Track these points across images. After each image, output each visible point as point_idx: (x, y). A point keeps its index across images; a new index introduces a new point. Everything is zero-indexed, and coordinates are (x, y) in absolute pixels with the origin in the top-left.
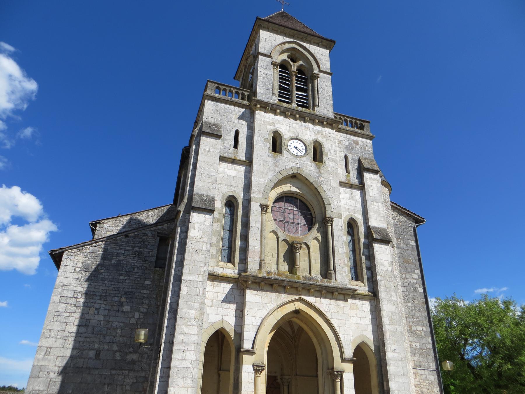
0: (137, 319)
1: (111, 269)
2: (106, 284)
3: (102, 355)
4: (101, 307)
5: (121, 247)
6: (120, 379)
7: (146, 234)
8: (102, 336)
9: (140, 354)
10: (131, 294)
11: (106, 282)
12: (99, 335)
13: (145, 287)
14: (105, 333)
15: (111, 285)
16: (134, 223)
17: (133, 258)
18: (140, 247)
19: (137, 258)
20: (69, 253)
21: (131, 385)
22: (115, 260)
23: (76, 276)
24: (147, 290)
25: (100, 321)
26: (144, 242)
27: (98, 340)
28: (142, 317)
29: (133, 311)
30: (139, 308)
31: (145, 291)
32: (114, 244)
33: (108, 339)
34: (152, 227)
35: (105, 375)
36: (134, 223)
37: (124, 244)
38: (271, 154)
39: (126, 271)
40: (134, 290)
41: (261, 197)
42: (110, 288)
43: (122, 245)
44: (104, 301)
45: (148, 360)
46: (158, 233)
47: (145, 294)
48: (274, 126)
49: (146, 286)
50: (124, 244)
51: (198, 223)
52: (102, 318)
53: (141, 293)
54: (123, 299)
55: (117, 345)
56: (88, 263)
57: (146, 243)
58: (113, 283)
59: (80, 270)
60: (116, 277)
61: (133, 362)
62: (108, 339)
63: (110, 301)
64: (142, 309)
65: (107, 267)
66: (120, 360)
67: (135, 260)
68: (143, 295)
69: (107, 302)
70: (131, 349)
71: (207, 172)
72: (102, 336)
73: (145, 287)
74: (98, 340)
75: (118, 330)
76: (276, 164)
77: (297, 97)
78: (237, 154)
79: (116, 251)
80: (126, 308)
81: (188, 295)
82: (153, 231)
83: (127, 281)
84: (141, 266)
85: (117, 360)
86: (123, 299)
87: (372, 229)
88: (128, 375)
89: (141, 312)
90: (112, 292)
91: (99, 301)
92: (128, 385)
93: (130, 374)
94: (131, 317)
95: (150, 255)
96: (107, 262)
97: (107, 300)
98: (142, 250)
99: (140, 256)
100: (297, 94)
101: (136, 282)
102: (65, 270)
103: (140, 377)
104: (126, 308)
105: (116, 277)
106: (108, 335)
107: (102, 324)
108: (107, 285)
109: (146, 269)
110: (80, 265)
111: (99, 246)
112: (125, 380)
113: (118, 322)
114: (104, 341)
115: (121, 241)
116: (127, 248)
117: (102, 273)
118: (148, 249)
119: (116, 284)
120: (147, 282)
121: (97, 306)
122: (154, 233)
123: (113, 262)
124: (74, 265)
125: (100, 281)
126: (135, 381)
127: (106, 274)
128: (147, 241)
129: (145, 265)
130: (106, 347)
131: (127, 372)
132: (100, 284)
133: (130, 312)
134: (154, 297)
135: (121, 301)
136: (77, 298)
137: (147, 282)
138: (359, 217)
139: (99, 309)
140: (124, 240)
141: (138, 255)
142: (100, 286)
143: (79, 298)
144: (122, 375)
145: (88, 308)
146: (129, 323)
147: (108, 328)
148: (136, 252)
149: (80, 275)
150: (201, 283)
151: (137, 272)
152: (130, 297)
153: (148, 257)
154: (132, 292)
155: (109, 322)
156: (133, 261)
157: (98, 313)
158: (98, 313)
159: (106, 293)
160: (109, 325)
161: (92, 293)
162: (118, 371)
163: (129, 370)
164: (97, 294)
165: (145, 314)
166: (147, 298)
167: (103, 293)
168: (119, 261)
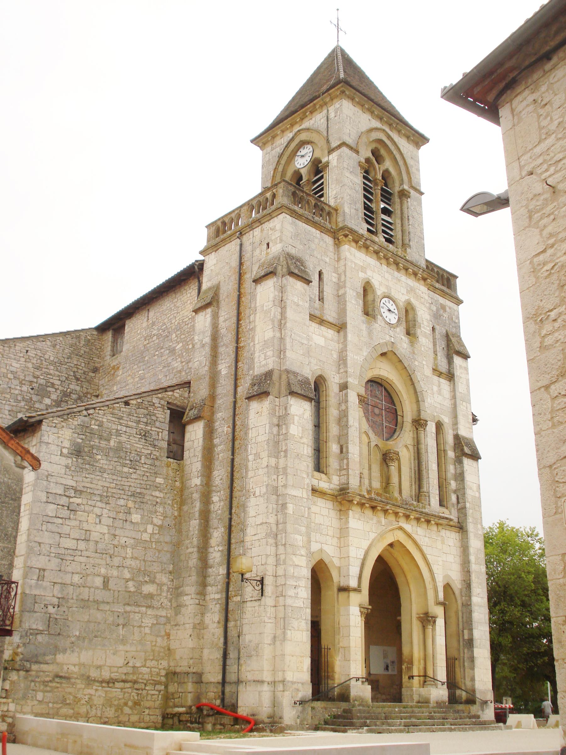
0: (151, 534)
1: (111, 454)
2: (106, 478)
3: (111, 585)
4: (104, 513)
5: (121, 421)
6: (137, 618)
7: (152, 404)
8: (108, 556)
9: (158, 585)
10: (140, 496)
11: (105, 475)
12: (104, 555)
13: (157, 487)
14: (111, 552)
15: (113, 480)
16: (34, 356)
17: (139, 441)
18: (146, 424)
19: (143, 441)
20: (51, 424)
21: (151, 627)
22: (115, 441)
23: (65, 461)
24: (160, 491)
25: (104, 534)
26: (150, 415)
27: (103, 562)
28: (157, 532)
29: (144, 522)
30: (152, 518)
31: (157, 494)
32: (111, 415)
33: (116, 561)
34: (160, 393)
35: (117, 611)
36: (34, 356)
37: (125, 415)
38: (364, 318)
39: (131, 461)
40: (143, 490)
41: (357, 383)
42: (113, 485)
43: (121, 418)
44: (107, 503)
45: (169, 593)
46: (168, 403)
47: (157, 497)
48: (365, 273)
49: (158, 485)
50: (125, 415)
51: (296, 415)
52: (105, 530)
53: (152, 495)
54: (130, 504)
55: (129, 572)
56: (78, 443)
57: (154, 418)
58: (115, 477)
59: (68, 453)
60: (119, 468)
61: (151, 596)
62: (116, 561)
63: (113, 506)
64: (155, 521)
65: (105, 451)
66: (134, 592)
67: (141, 443)
68: (155, 498)
69: (110, 506)
70: (147, 577)
71: (298, 338)
72: (108, 556)
73: (157, 487)
74: (103, 562)
75: (128, 549)
76: (370, 333)
77: (383, 225)
78: (323, 310)
79: (114, 427)
80: (136, 517)
81: (295, 516)
82: (161, 399)
83: (134, 476)
84: (150, 454)
85: (130, 592)
86: (130, 504)
87: (461, 440)
88: (146, 614)
89: (155, 525)
90: (114, 491)
91: (99, 504)
92: (147, 627)
93: (149, 613)
94: (143, 531)
95: (160, 437)
96: (104, 443)
97: (109, 504)
98: (149, 428)
99: (147, 438)
100: (383, 220)
101: (145, 478)
102: (47, 450)
103: (161, 616)
104: (136, 517)
105: (119, 468)
106: (116, 556)
107: (106, 538)
108: (108, 480)
109: (157, 459)
110: (67, 444)
111: (91, 416)
112: (143, 621)
113: (127, 537)
114: (112, 564)
115: (120, 410)
116: (130, 423)
117: (99, 459)
118: (156, 427)
119: (120, 479)
120: (159, 480)
121: (97, 511)
122: (163, 402)
123: (112, 443)
124: (60, 444)
125: (98, 473)
126: (155, 622)
127: (105, 462)
128: (155, 415)
129: (154, 453)
130: (115, 573)
131: (144, 609)
132: (98, 477)
133: (142, 523)
134: (169, 504)
135: (128, 506)
136: (69, 497)
137: (159, 480)
138: (446, 420)
139: (100, 516)
140: (124, 410)
141: (145, 435)
142: (99, 480)
143: (72, 497)
144: (139, 613)
145: (86, 514)
146: (141, 539)
147: (115, 546)
148: (142, 431)
149: (69, 461)
150: (305, 500)
151: (145, 463)
152: (139, 500)
153: (158, 440)
154: (140, 493)
155: (115, 536)
156: (138, 446)
157: (100, 521)
158: (100, 521)
159: (107, 492)
160: (116, 542)
161: (89, 491)
162: (134, 607)
163: (147, 607)
164: (96, 492)
165: (161, 527)
166: (161, 504)
167: (104, 492)
168: (120, 442)
